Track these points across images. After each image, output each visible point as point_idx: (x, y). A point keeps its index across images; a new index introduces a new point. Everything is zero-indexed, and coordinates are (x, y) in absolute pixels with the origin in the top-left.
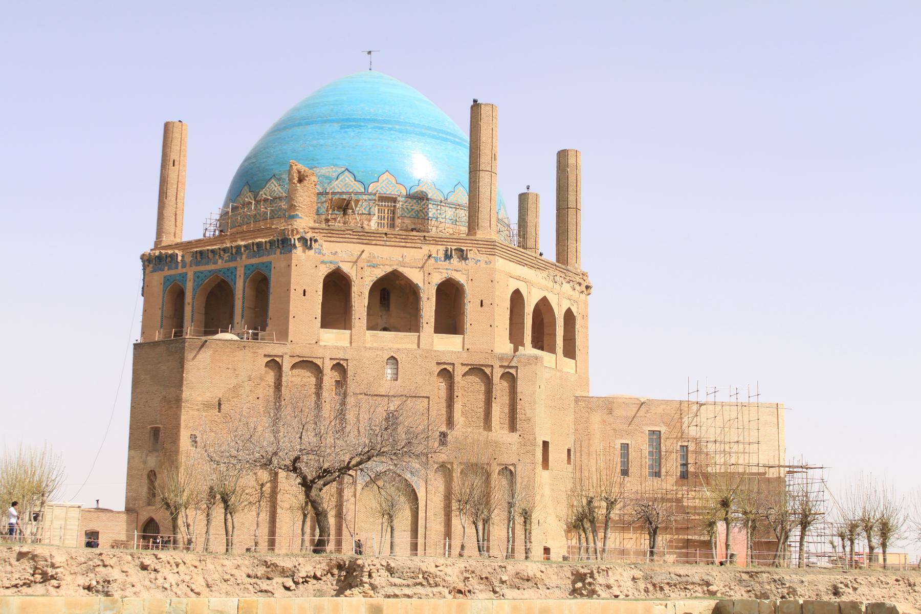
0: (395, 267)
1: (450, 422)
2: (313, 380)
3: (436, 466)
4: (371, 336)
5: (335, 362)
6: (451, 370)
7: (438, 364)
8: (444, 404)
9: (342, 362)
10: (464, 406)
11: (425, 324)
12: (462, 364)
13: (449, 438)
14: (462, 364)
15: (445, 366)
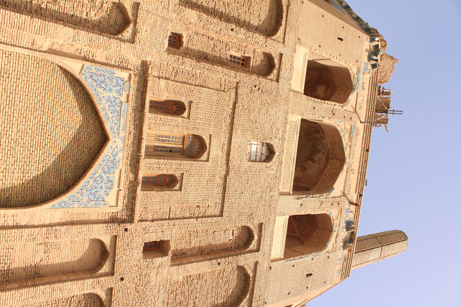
0: (347, 160)
1: (180, 257)
2: (255, 22)
3: (107, 241)
4: (295, 122)
5: (276, 61)
6: (251, 247)
7: (261, 225)
8: (204, 244)
9: (275, 72)
10: (199, 277)
11: (300, 201)
12: (257, 263)
13: (158, 260)
14: (256, 263)
15: (256, 238)
